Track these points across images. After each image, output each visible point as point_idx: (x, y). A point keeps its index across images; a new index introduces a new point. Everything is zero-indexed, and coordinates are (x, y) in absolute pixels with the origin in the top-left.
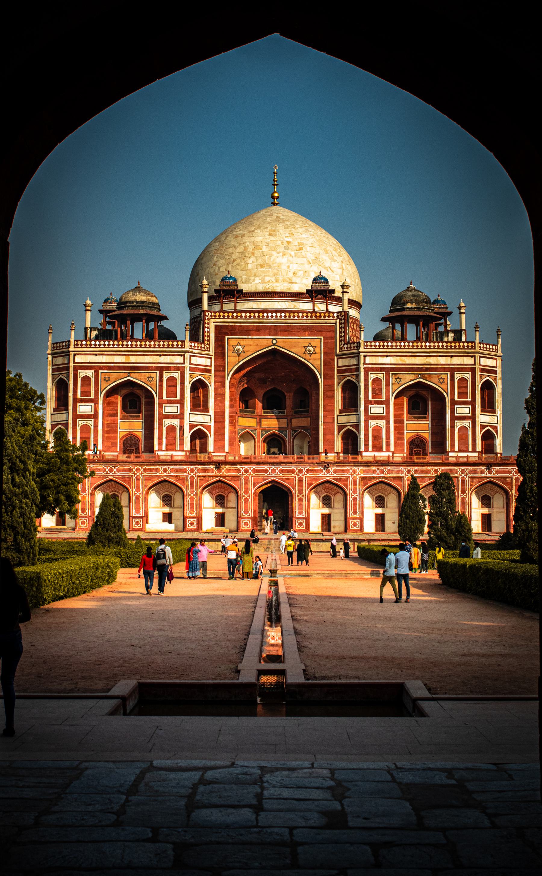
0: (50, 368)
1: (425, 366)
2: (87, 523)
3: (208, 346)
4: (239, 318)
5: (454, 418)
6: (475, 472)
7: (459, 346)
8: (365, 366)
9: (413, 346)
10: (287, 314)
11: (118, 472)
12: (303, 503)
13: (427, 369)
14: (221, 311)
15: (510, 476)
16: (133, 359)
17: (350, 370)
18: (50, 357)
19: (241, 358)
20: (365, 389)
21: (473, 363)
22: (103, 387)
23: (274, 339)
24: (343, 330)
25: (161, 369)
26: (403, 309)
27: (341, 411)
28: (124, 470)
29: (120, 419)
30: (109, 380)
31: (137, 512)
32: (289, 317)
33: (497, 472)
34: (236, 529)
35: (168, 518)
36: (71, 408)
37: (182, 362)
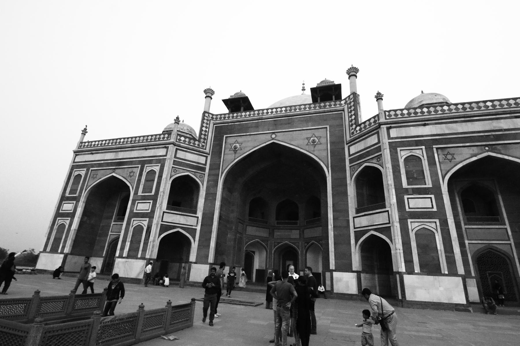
1: (494, 133)
3: (204, 144)
8: (390, 141)
10: (288, 109)
16: (122, 155)
17: (368, 154)
19: (237, 155)
20: (394, 172)
23: (273, 133)
24: (353, 113)
25: (143, 163)
27: (358, 211)
29: (114, 222)
30: (96, 177)
32: (290, 110)
37: (165, 154)
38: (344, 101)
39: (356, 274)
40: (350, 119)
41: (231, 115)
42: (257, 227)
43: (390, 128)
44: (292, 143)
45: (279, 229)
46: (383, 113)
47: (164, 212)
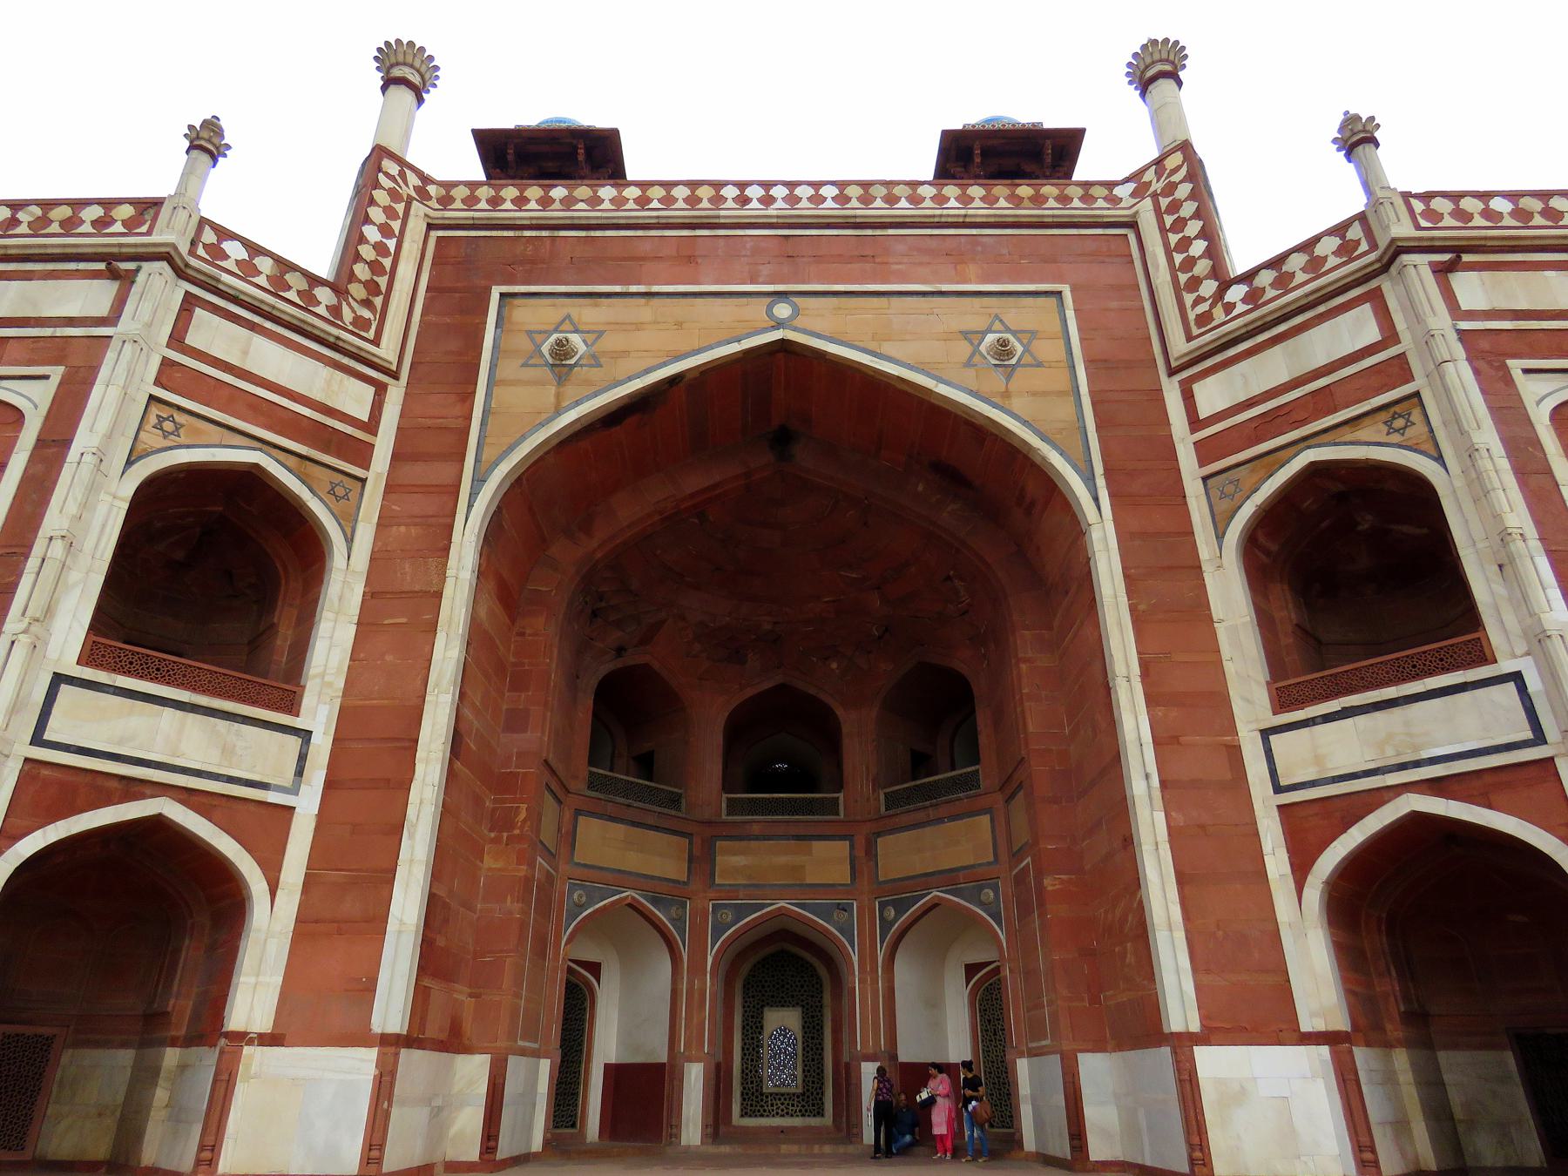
3: (367, 314)
4: (581, 206)
8: (1464, 325)
19: (571, 391)
24: (1193, 228)
27: (1283, 700)
32: (866, 200)
37: (103, 310)
38: (1131, 186)
39: (1325, 1050)
40: (1178, 258)
41: (534, 192)
42: (635, 824)
43: (1451, 267)
44: (887, 348)
45: (740, 838)
46: (1399, 202)
47: (58, 679)
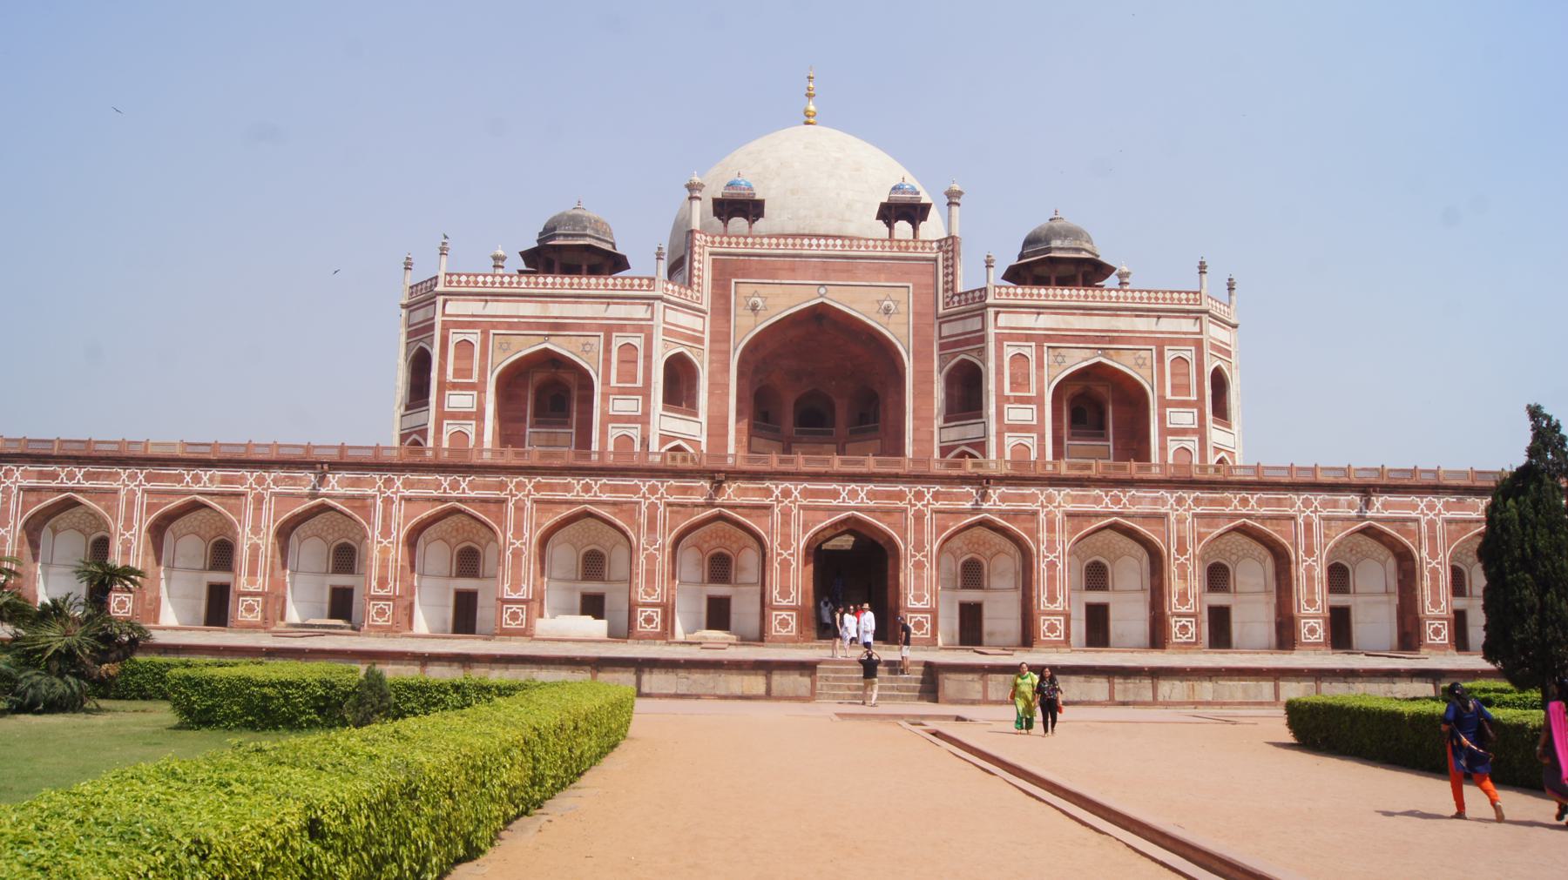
0: (403, 331)
2: (389, 613)
5: (1165, 432)
6: (1335, 505)
7: (1172, 299)
9: (1086, 296)
11: (472, 489)
12: (926, 573)
13: (1113, 340)
14: (725, 234)
15: (1414, 515)
16: (556, 310)
17: (967, 342)
18: (404, 312)
19: (759, 319)
21: (1197, 329)
22: (498, 359)
25: (609, 330)
26: (1049, 250)
27: (946, 421)
28: (486, 487)
31: (516, 587)
33: (1385, 506)
34: (756, 634)
35: (593, 606)
36: (433, 398)
